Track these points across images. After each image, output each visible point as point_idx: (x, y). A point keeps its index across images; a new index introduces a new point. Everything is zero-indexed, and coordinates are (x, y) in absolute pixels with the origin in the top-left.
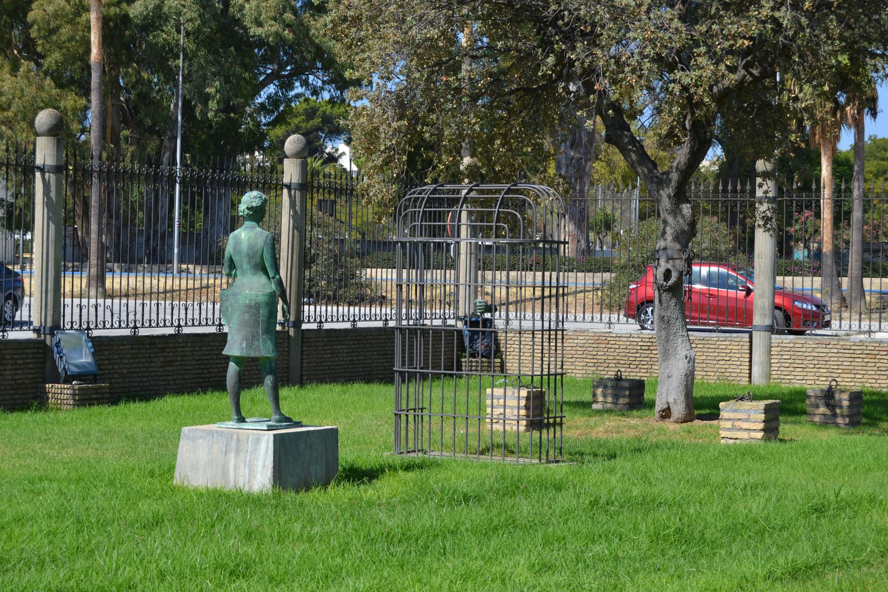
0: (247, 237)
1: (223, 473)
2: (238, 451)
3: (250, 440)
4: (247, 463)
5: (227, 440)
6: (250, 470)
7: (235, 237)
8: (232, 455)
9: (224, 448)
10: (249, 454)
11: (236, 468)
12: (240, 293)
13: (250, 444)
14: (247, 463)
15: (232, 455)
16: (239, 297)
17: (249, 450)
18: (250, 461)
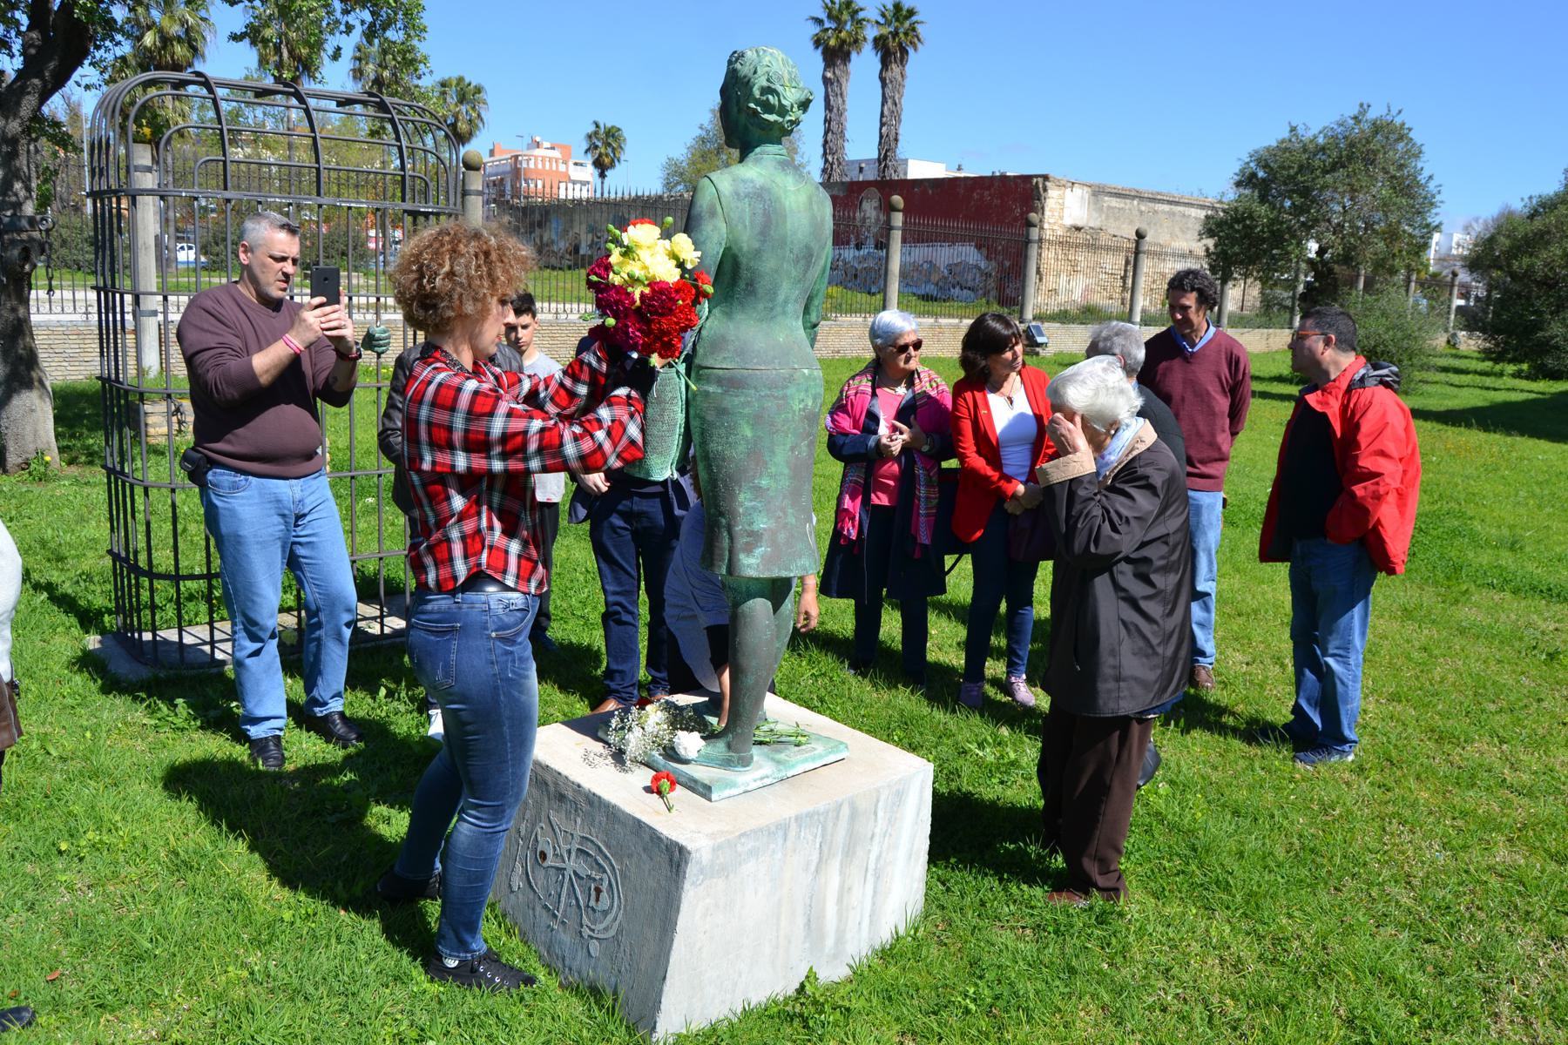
0: (803, 198)
1: (808, 923)
2: (849, 852)
3: (880, 804)
4: (872, 866)
5: (824, 829)
6: (877, 878)
7: (761, 195)
8: (835, 865)
9: (815, 857)
10: (877, 839)
11: (844, 891)
12: (791, 379)
13: (880, 814)
14: (872, 866)
15: (835, 865)
16: (791, 391)
17: (877, 830)
18: (879, 858)
